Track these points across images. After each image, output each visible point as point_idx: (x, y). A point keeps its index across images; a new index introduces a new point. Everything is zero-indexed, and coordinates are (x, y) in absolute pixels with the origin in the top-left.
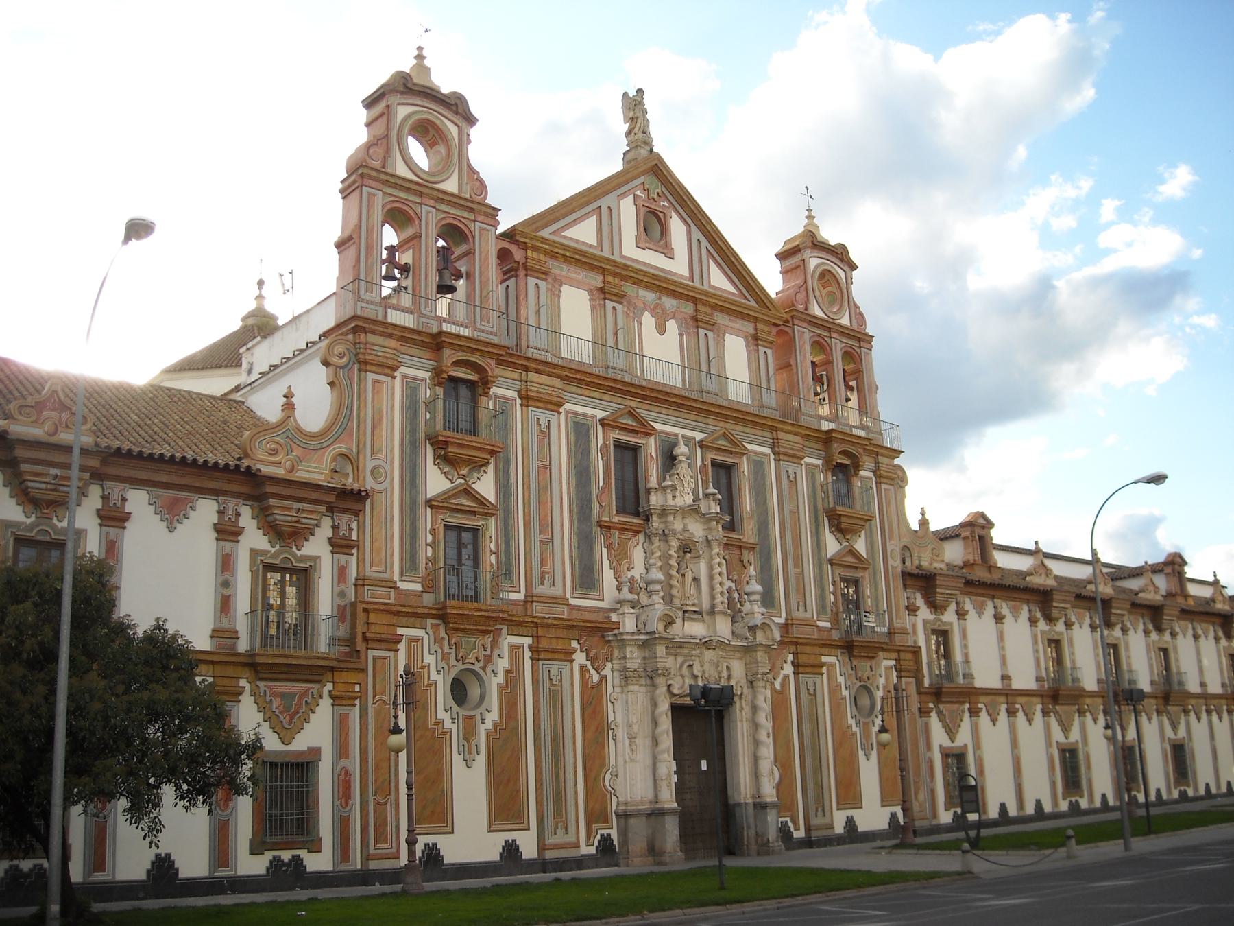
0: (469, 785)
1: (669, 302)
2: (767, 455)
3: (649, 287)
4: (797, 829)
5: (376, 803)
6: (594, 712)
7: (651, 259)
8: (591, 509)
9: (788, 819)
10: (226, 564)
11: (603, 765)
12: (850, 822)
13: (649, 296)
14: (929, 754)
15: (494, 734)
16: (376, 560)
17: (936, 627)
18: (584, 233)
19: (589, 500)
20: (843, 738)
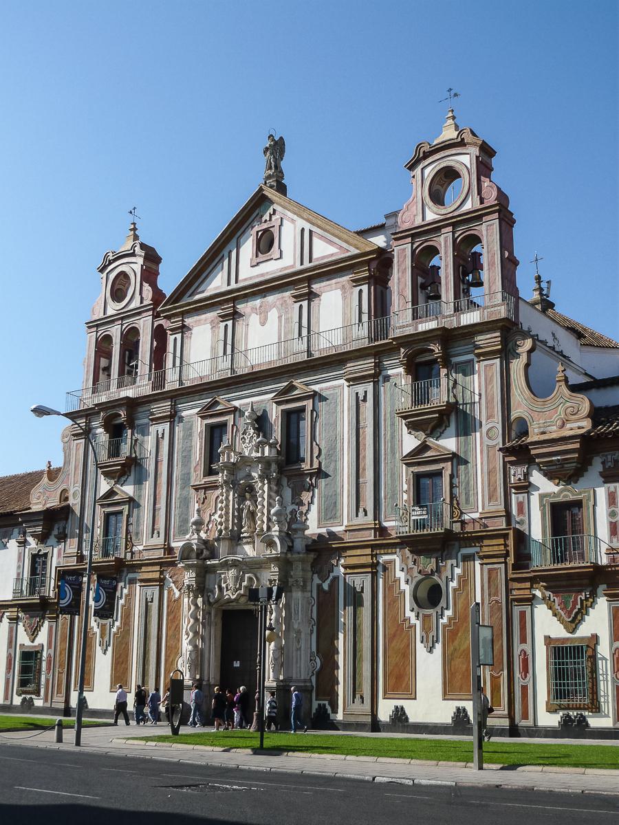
0: (103, 664)
1: (271, 299)
2: (341, 386)
3: (254, 295)
4: (335, 711)
5: (59, 673)
6: (174, 617)
7: (270, 269)
8: (189, 479)
9: (327, 702)
10: (21, 558)
11: (177, 653)
12: (399, 717)
13: (257, 302)
14: (527, 647)
15: (117, 634)
16: (72, 544)
17: (560, 499)
18: (217, 284)
19: (189, 474)
20: (400, 631)
